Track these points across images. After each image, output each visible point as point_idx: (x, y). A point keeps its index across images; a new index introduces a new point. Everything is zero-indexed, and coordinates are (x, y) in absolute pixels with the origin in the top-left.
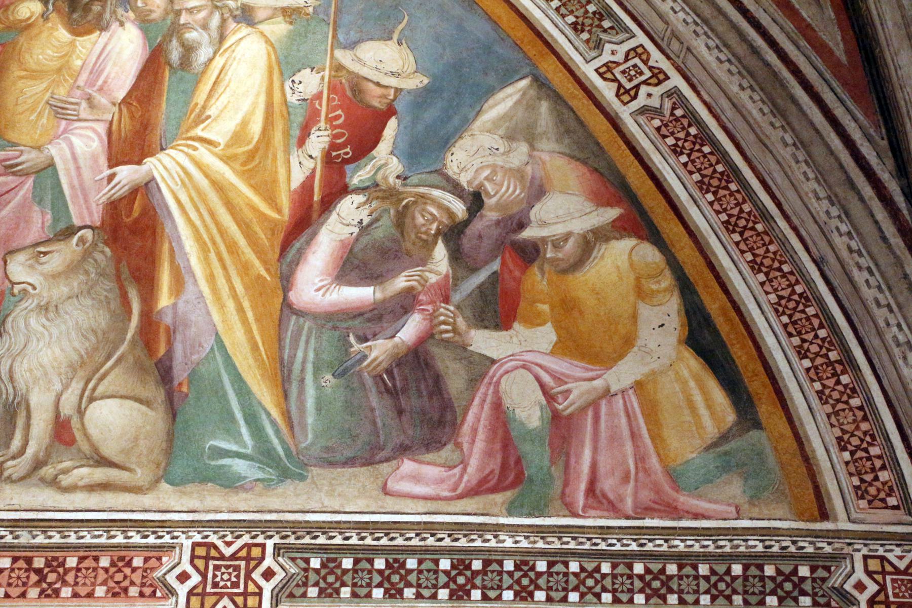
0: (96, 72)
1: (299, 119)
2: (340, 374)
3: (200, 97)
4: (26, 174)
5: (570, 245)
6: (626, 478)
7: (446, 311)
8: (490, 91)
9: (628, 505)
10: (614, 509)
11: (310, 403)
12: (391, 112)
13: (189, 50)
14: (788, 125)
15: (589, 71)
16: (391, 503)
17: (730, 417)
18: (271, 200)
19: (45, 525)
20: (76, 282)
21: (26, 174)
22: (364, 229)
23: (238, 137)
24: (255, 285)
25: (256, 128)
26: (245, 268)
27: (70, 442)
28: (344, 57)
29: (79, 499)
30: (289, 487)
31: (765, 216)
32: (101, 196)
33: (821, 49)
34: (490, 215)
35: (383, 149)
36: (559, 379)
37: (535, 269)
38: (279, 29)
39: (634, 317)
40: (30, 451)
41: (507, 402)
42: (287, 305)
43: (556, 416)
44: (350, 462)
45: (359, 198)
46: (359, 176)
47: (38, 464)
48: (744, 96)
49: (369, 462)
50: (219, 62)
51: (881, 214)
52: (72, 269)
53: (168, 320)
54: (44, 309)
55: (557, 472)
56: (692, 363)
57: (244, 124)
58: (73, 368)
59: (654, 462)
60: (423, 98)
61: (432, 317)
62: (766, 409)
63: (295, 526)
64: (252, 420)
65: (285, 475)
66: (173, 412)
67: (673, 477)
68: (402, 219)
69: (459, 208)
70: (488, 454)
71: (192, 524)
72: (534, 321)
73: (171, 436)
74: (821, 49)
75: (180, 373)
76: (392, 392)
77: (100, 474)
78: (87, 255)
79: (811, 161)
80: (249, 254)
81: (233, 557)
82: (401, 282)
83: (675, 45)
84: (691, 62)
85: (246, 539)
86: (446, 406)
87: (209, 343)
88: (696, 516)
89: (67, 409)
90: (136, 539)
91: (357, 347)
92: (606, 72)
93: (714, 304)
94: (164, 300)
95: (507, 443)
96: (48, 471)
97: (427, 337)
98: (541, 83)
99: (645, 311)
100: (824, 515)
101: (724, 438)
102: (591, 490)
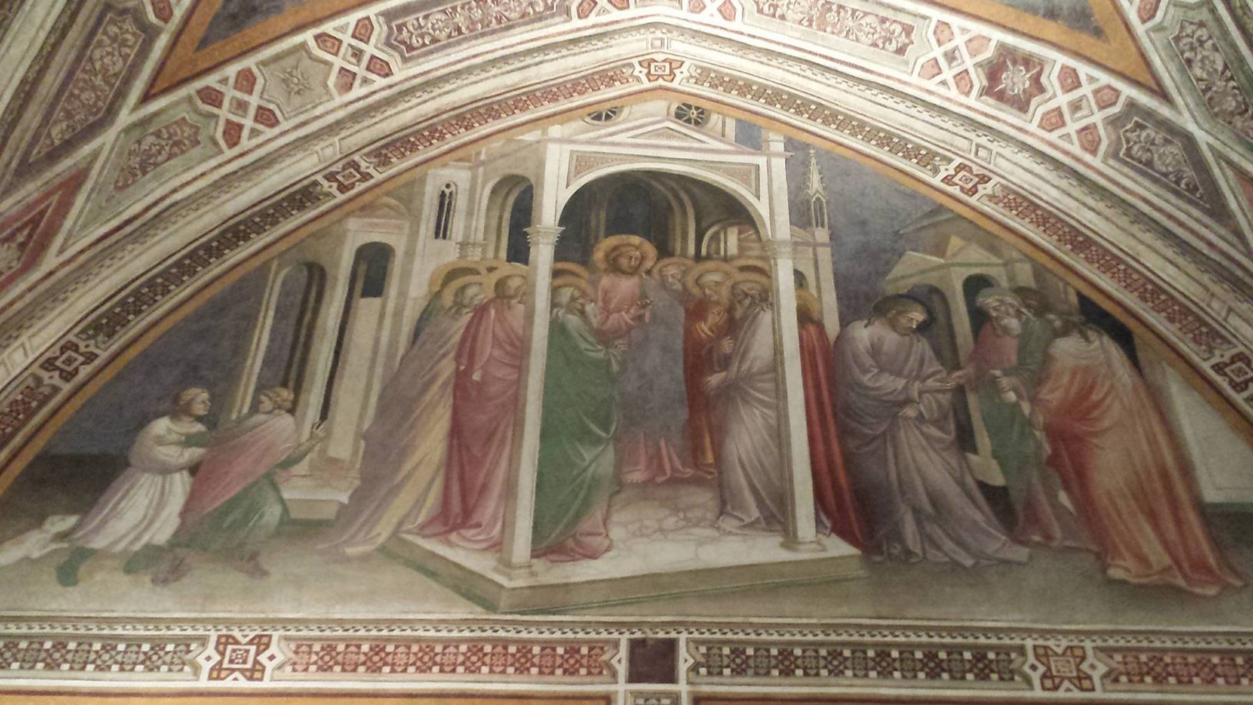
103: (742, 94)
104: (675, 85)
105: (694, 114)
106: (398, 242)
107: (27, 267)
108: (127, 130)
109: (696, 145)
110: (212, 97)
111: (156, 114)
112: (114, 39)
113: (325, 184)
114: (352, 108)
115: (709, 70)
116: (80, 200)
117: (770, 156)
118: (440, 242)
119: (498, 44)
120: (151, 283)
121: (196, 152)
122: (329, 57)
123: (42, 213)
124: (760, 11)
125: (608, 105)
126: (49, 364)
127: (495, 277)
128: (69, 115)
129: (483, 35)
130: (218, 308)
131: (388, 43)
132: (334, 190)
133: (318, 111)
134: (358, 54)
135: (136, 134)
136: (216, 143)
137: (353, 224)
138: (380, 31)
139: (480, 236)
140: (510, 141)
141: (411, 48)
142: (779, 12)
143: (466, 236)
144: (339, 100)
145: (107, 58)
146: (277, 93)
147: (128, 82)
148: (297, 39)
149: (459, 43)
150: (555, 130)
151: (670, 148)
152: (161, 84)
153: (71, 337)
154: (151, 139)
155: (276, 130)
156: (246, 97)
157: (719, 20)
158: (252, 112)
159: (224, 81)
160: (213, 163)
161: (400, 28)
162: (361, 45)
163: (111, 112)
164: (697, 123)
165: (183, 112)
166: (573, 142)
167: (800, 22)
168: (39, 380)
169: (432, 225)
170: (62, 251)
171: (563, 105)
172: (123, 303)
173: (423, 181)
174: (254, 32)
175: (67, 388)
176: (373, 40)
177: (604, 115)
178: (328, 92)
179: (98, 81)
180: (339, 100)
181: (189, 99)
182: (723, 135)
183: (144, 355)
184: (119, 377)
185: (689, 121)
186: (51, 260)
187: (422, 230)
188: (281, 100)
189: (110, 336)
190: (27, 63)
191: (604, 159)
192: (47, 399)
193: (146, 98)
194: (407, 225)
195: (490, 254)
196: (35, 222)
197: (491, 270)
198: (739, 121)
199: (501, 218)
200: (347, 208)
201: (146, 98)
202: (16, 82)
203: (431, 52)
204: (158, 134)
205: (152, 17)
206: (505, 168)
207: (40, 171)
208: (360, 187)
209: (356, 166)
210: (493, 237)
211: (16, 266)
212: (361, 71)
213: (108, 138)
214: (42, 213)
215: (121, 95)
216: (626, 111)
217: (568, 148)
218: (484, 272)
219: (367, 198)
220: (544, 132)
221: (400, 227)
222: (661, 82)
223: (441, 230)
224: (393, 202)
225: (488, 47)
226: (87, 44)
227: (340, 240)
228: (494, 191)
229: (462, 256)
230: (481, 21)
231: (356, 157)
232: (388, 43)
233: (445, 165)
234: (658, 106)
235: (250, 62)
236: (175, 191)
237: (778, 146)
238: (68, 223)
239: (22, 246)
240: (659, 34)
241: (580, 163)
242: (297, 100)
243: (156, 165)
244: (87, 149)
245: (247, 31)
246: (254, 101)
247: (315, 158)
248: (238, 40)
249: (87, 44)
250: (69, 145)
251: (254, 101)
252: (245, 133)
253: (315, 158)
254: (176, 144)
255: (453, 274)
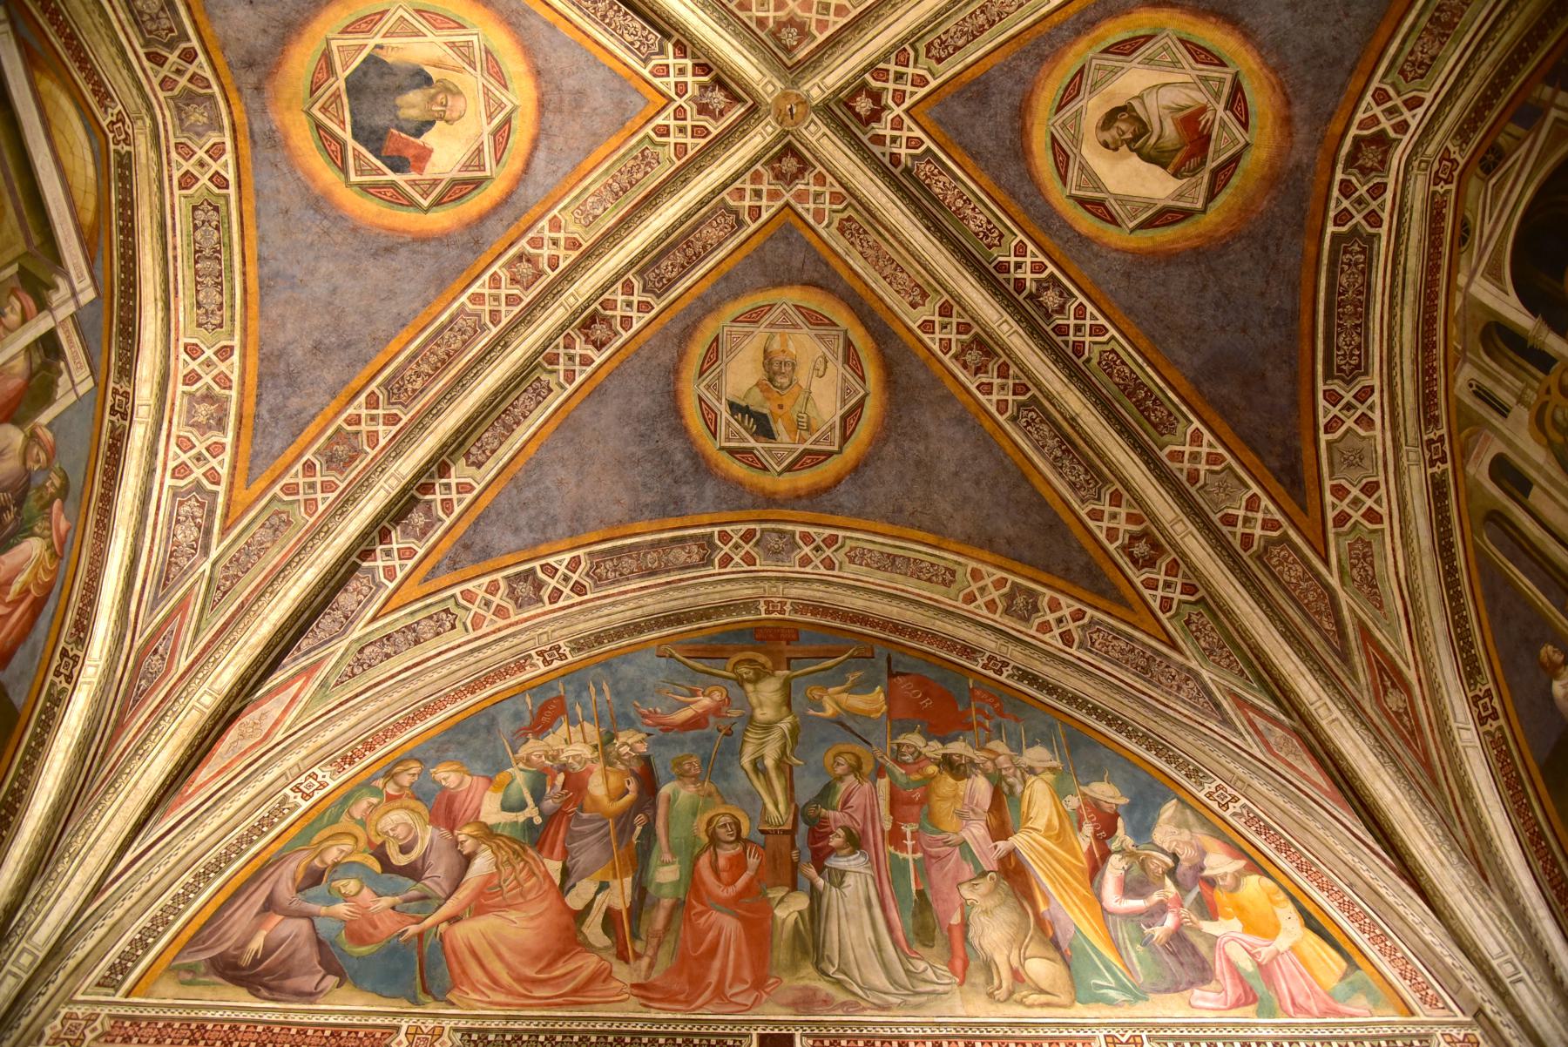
0: (972, 797)
1: (1075, 818)
2: (1145, 945)
3: (1024, 808)
4: (954, 846)
5: (1229, 879)
6: (1308, 997)
7: (1184, 911)
8: (1160, 806)
9: (1315, 1011)
10: (1308, 1013)
11: (1135, 960)
12: (1116, 815)
13: (1011, 787)
14: (1315, 819)
15: (1201, 795)
16: (1197, 1013)
17: (1344, 964)
18: (1076, 857)
19: (1026, 1025)
20: (996, 899)
21: (954, 846)
22: (1127, 871)
23: (1049, 826)
24: (1084, 899)
25: (1056, 822)
26: (1076, 892)
27: (1023, 981)
28: (1085, 789)
29: (1037, 1011)
30: (1141, 1004)
31: (1313, 864)
32: (994, 856)
33: (1315, 784)
34: (1184, 865)
35: (1120, 832)
36: (1253, 947)
37: (1217, 890)
38: (1049, 777)
39: (1275, 914)
40: (1005, 985)
41: (1233, 959)
42: (1103, 909)
43: (1259, 965)
44: (1167, 991)
45: (1118, 856)
46: (1114, 846)
47: (1011, 993)
48: (1288, 806)
49: (1177, 991)
50: (1027, 792)
51: (1378, 861)
52: (992, 892)
53: (1048, 917)
54: (985, 912)
55: (1272, 994)
56: (1313, 938)
57: (1050, 820)
58: (1011, 942)
59: (1317, 987)
60: (1130, 808)
61: (1178, 915)
62: (1358, 959)
63: (1152, 1025)
64: (1109, 969)
65: (1137, 998)
66: (1068, 967)
67: (1331, 996)
68: (1143, 865)
69: (1169, 861)
70: (1235, 985)
71: (1100, 1025)
72: (1228, 917)
73: (1071, 977)
74: (1315, 784)
75: (1064, 946)
76: (1173, 953)
77: (1044, 998)
78: (997, 885)
79: (1333, 836)
80: (1075, 884)
81: (1127, 1042)
82: (1156, 897)
83: (1239, 784)
84: (1250, 792)
85: (1130, 1033)
86: (1203, 961)
87: (1073, 929)
88: (1352, 1016)
89: (1015, 964)
90: (1074, 1033)
91: (1147, 931)
92: (1209, 795)
93: (1310, 908)
94: (1043, 908)
95: (1242, 980)
96: (1016, 996)
97: (1179, 925)
98: (1180, 800)
99: (1279, 912)
100: (1412, 1014)
101: (1345, 976)
102: (1294, 1003)
103: (1490, 107)
104: (1462, 162)
105: (1490, 157)
106: (1497, 447)
107: (1408, 689)
108: (1343, 584)
109: (1517, 166)
110: (1342, 519)
111: (1339, 561)
112: (1281, 564)
113: (1435, 469)
114: (1387, 425)
115: (1461, 127)
116: (1378, 634)
117: (1551, 103)
118: (1510, 416)
119: (1379, 298)
120: (1456, 625)
121: (1375, 547)
122: (1343, 428)
123: (1377, 662)
124: (1422, 76)
125: (1458, 227)
126: (1482, 721)
127: (1555, 390)
128: (1319, 613)
129: (1367, 308)
130: (1492, 596)
131: (1348, 383)
132: (1443, 467)
133: (1380, 451)
134: (1349, 407)
135: (1347, 579)
136: (1375, 531)
137: (1471, 470)
138: (1337, 386)
139: (1518, 383)
140: (1455, 319)
141: (1358, 366)
142: (1427, 61)
143: (1515, 395)
144: (1378, 432)
145: (1292, 573)
146: (1356, 474)
147: (1311, 568)
148: (1323, 445)
149: (1367, 328)
150: (1462, 280)
151: (1511, 191)
152: (1321, 548)
153: (1470, 695)
154: (1355, 572)
155: (1383, 486)
156: (1351, 497)
157: (1420, 111)
158: (1363, 497)
159: (1334, 506)
160: (1388, 539)
161: (1340, 370)
162: (1343, 402)
163: (1327, 587)
164: (1500, 158)
165: (1345, 543)
166: (1475, 270)
167: (1442, 44)
168: (1487, 733)
169: (1495, 414)
170: (1408, 666)
171: (1445, 262)
172: (1462, 650)
173: (1459, 400)
174: (1309, 474)
175: (1502, 721)
176: (1342, 392)
177: (1464, 233)
178: (1369, 438)
179: (1304, 585)
180: (1378, 432)
181: (1337, 535)
182: (1518, 139)
183: (1502, 663)
184: (1510, 687)
185: (1495, 165)
186: (1411, 675)
187: (1496, 423)
188: (1363, 473)
189: (1480, 673)
190: (1272, 628)
191: (1498, 251)
192: (1504, 737)
193: (1326, 562)
194: (1487, 432)
195: (1536, 385)
196: (1381, 669)
197: (1548, 391)
198: (1512, 120)
199: (1512, 361)
200: (1458, 465)
201: (1326, 562)
202: (1281, 640)
203: (1367, 351)
204: (1353, 566)
205: (1275, 534)
206: (1473, 337)
207: (1349, 648)
208: (1447, 447)
209: (1430, 442)
210: (1524, 375)
211: (1405, 696)
212: (1362, 409)
213: (1343, 597)
214: (1377, 662)
215: (1318, 576)
216: (1468, 214)
217: (1478, 277)
218: (1547, 398)
219: (1456, 447)
220: (1459, 289)
221: (1487, 438)
222: (1456, 174)
223: (1503, 411)
224: (1466, 432)
225: (1378, 306)
226: (1279, 582)
227: (1479, 485)
228: (1489, 354)
229: (1528, 406)
230: (1356, 307)
231: (1425, 438)
232: (1348, 383)
233: (1455, 380)
234: (1473, 185)
235: (1327, 484)
236: (1397, 574)
237: (1548, 91)
238: (1391, 650)
239: (1393, 685)
240: (1416, 164)
241: (1493, 274)
242: (1366, 463)
243: (1374, 577)
244: (1346, 613)
245: (1306, 476)
246: (1355, 492)
247: (1414, 468)
248: (1310, 485)
249: (1279, 582)
250: (1339, 622)
251: (1355, 492)
252: (1376, 507)
253: (1414, 468)
254: (1365, 556)
255: (1539, 421)
